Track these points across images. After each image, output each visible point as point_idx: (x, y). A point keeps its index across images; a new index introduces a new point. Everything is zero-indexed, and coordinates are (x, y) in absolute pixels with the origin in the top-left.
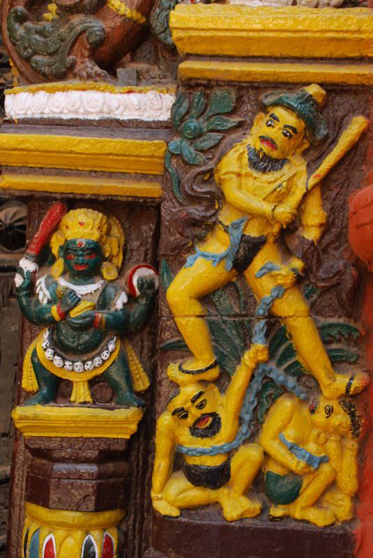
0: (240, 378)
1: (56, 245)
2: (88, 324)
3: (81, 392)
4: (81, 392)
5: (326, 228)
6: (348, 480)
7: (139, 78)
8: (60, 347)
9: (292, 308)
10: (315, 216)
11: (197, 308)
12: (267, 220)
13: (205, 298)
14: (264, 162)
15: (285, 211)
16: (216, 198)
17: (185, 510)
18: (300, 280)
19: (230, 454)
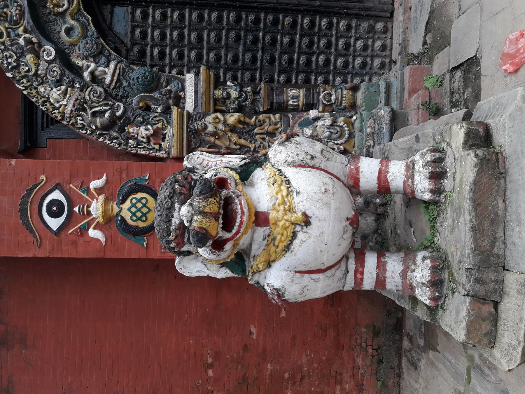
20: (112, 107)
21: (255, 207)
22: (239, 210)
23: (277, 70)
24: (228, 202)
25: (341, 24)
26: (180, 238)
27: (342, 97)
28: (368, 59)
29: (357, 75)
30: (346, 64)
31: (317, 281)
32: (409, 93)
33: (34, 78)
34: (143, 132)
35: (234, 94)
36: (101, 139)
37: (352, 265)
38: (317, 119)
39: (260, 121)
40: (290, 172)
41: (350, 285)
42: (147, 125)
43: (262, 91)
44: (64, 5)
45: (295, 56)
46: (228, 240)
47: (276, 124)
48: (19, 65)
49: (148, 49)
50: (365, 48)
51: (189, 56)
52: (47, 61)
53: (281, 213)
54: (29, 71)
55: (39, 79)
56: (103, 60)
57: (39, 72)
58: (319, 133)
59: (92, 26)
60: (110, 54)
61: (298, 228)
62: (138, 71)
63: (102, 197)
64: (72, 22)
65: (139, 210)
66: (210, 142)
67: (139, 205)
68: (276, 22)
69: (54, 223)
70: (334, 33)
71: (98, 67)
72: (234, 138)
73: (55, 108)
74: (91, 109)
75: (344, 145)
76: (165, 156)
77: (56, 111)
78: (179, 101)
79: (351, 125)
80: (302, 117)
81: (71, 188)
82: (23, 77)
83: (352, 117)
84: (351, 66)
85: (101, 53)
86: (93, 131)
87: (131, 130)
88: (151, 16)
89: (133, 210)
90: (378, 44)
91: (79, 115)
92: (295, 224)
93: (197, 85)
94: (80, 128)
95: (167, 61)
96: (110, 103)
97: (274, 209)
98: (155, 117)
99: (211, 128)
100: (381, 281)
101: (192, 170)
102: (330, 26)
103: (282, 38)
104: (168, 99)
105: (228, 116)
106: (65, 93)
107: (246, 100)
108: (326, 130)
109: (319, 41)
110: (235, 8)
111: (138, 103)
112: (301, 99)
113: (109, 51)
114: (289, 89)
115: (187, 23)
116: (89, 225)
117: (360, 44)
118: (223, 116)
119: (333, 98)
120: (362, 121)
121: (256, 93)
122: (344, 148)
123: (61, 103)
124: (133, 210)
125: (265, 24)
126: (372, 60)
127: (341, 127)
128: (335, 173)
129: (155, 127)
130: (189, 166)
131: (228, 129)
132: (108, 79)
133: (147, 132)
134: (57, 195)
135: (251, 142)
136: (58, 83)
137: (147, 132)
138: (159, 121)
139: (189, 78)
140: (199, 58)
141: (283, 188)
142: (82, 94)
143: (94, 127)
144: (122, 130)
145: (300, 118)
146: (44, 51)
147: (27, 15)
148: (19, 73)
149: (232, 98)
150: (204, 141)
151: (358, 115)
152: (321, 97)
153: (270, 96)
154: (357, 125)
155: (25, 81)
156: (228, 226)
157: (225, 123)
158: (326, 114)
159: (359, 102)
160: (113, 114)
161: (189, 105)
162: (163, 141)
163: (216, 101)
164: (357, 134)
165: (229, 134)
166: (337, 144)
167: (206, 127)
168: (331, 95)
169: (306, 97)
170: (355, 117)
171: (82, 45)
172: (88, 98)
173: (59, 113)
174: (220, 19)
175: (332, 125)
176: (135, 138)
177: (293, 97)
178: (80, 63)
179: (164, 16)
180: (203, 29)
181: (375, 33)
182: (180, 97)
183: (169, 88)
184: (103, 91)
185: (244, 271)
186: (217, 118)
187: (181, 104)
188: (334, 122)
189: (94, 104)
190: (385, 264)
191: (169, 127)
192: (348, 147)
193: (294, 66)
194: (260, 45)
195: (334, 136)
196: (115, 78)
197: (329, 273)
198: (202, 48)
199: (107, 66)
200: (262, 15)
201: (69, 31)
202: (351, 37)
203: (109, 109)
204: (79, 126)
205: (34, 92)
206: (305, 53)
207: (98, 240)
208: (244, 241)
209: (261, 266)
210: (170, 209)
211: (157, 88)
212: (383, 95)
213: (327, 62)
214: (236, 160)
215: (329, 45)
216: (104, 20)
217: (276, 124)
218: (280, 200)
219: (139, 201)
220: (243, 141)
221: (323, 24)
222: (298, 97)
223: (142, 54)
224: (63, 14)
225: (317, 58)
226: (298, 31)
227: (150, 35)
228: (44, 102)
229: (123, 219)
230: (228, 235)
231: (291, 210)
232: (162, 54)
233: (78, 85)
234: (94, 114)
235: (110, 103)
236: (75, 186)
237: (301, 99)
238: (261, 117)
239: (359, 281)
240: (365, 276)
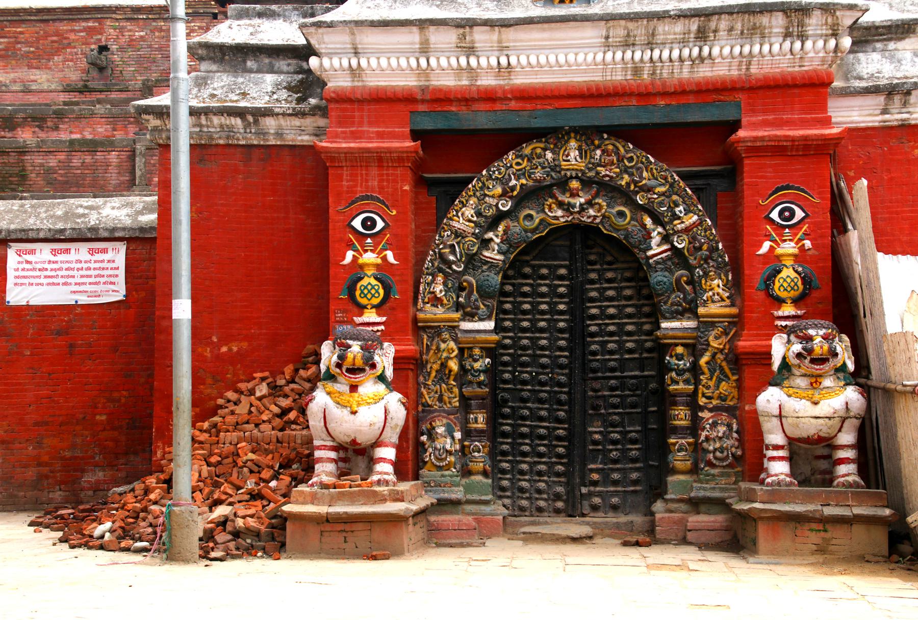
0: (714, 379)
1: (673, 354)
2: (683, 369)
3: (681, 383)
4: (681, 383)
5: (729, 349)
6: (736, 396)
7: (689, 318)
8: (678, 375)
9: (724, 364)
10: (727, 347)
11: (705, 365)
12: (718, 349)
13: (707, 363)
14: (716, 338)
15: (721, 347)
16: (708, 345)
17: (705, 403)
18: (725, 359)
19: (713, 393)
20: (459, 261)
21: (361, 385)
22: (357, 376)
23: (513, 405)
24: (363, 370)
25: (560, 467)
26: (341, 345)
27: (477, 462)
28: (528, 495)
29: (512, 483)
30: (522, 473)
31: (320, 422)
32: (475, 519)
33: (482, 192)
34: (439, 288)
35: (477, 365)
36: (431, 253)
37: (331, 444)
38: (453, 438)
39: (451, 388)
40: (381, 405)
41: (317, 443)
42: (445, 291)
43: (479, 390)
44: (552, 212)
45: (528, 423)
46: (341, 370)
47: (450, 403)
48: (493, 180)
49: (531, 281)
50: (539, 491)
51: (525, 320)
52: (497, 204)
53: (357, 399)
54: (488, 188)
55: (482, 197)
56: (504, 247)
57: (487, 198)
58: (439, 441)
59: (537, 236)
60: (512, 254)
61: (349, 409)
62: (496, 279)
63: (379, 261)
64: (537, 221)
65: (369, 292)
66: (432, 345)
67: (373, 291)
68: (560, 402)
69: (357, 223)
70: (554, 460)
71: (498, 245)
72: (436, 367)
73: (457, 212)
74: (458, 243)
75: (430, 462)
76: (419, 307)
77: (455, 213)
78: (470, 316)
79: (448, 467)
80: (456, 426)
81: (386, 235)
82: (483, 183)
83: (455, 468)
84: (519, 477)
85: (511, 246)
86: (438, 245)
87: (439, 278)
88: (560, 283)
89: (369, 287)
90: (542, 504)
91: (452, 233)
92: (351, 407)
93: (485, 331)
94: (440, 234)
95: (519, 299)
96: (464, 259)
97: (360, 395)
98: (452, 298)
99: (443, 346)
100: (320, 460)
101: (382, 348)
102: (559, 456)
103: (545, 409)
104: (471, 307)
105: (455, 360)
106: (470, 221)
107: (472, 375)
108: (442, 445)
109: (544, 445)
110: (570, 363)
111: (465, 281)
112: (475, 426)
113: (513, 252)
114: (485, 415)
115: (555, 317)
116: (356, 251)
117: (542, 485)
118: (456, 356)
119: (476, 454)
120: (451, 476)
121: (480, 384)
122: (427, 462)
123: (461, 218)
124: (369, 287)
125: (556, 392)
126: (527, 498)
127: (446, 459)
128: (384, 433)
129: (444, 298)
130: (384, 347)
131: (443, 360)
132: (486, 254)
133: (438, 292)
134: (380, 224)
135: (433, 381)
136: (479, 214)
137: (438, 292)
138: (449, 301)
139: (490, 325)
140: (524, 330)
141: (371, 401)
142: (470, 235)
143: (441, 247)
144: (440, 270)
145: (455, 424)
146: (507, 201)
147: (537, 184)
148: (487, 180)
149: (473, 363)
150: (433, 340)
151: (456, 473)
152: (476, 443)
153: (477, 397)
154: (447, 473)
155: (480, 185)
156: (348, 370)
157: (448, 358)
158: (458, 447)
159: (473, 477)
160: (454, 262)
161: (466, 325)
162: (432, 305)
163: (470, 349)
164: (440, 473)
165: (439, 362)
166: (430, 456)
167: (444, 342)
168: (479, 452)
169: (476, 430)
170: (454, 470)
171: (517, 230)
172: (467, 239)
173: (454, 216)
174: (561, 349)
175: (447, 451)
176: (433, 281)
177: (476, 419)
178: (501, 228)
179: (561, 296)
180: (550, 332)
181: (554, 501)
182: (474, 317)
183: (482, 306)
184: (474, 252)
185: (325, 380)
186: (453, 351)
187: (468, 318)
188: (450, 453)
189: (461, 245)
190: (332, 462)
191: (443, 310)
192: (428, 465)
193: (520, 422)
194: (537, 388)
195: (437, 453)
196: (489, 260)
197: (324, 429)
198: (532, 333)
199: (499, 252)
200: (566, 390)
201: (529, 217)
202: (549, 477)
203: (457, 258)
204: (442, 233)
205: (471, 193)
206: (531, 432)
207: (344, 258)
208: (340, 379)
209: (327, 389)
210: (358, 340)
211: (481, 296)
212: (476, 497)
213: (524, 454)
214: (389, 373)
215: (541, 455)
216: (555, 240)
217: (450, 403)
218: (364, 398)
219: (377, 292)
220: (434, 374)
221: (560, 449)
222: (476, 422)
223: (526, 276)
224: (543, 211)
225: (527, 444)
226: (552, 425)
227: (542, 282)
228: (463, 202)
229: (361, 279)
230: (344, 372)
231: (359, 405)
232: (525, 295)
233: (477, 231)
234: (453, 246)
235: (464, 259)
236: (387, 240)
237: (475, 426)
238: (456, 390)
239: (319, 448)
240: (323, 452)
